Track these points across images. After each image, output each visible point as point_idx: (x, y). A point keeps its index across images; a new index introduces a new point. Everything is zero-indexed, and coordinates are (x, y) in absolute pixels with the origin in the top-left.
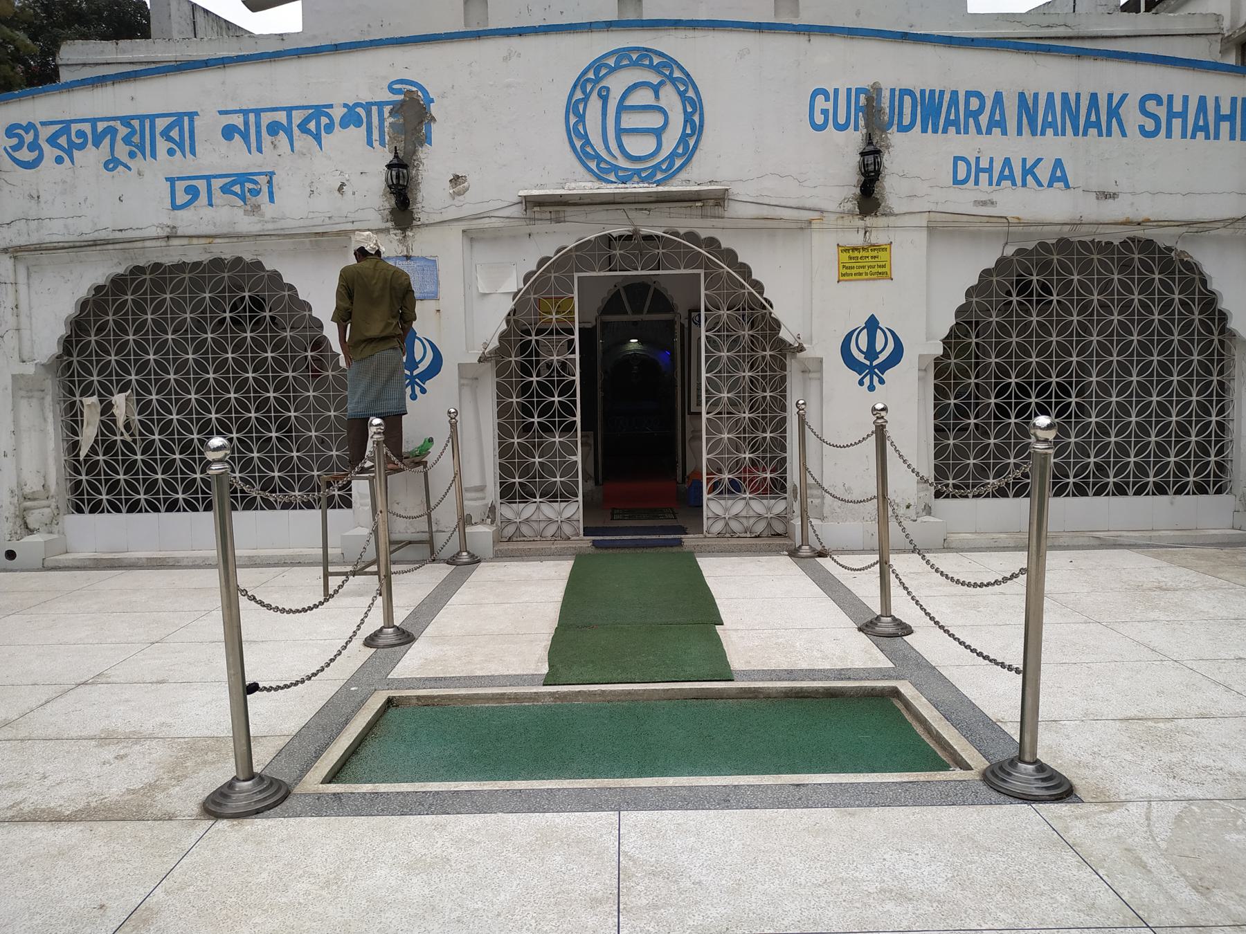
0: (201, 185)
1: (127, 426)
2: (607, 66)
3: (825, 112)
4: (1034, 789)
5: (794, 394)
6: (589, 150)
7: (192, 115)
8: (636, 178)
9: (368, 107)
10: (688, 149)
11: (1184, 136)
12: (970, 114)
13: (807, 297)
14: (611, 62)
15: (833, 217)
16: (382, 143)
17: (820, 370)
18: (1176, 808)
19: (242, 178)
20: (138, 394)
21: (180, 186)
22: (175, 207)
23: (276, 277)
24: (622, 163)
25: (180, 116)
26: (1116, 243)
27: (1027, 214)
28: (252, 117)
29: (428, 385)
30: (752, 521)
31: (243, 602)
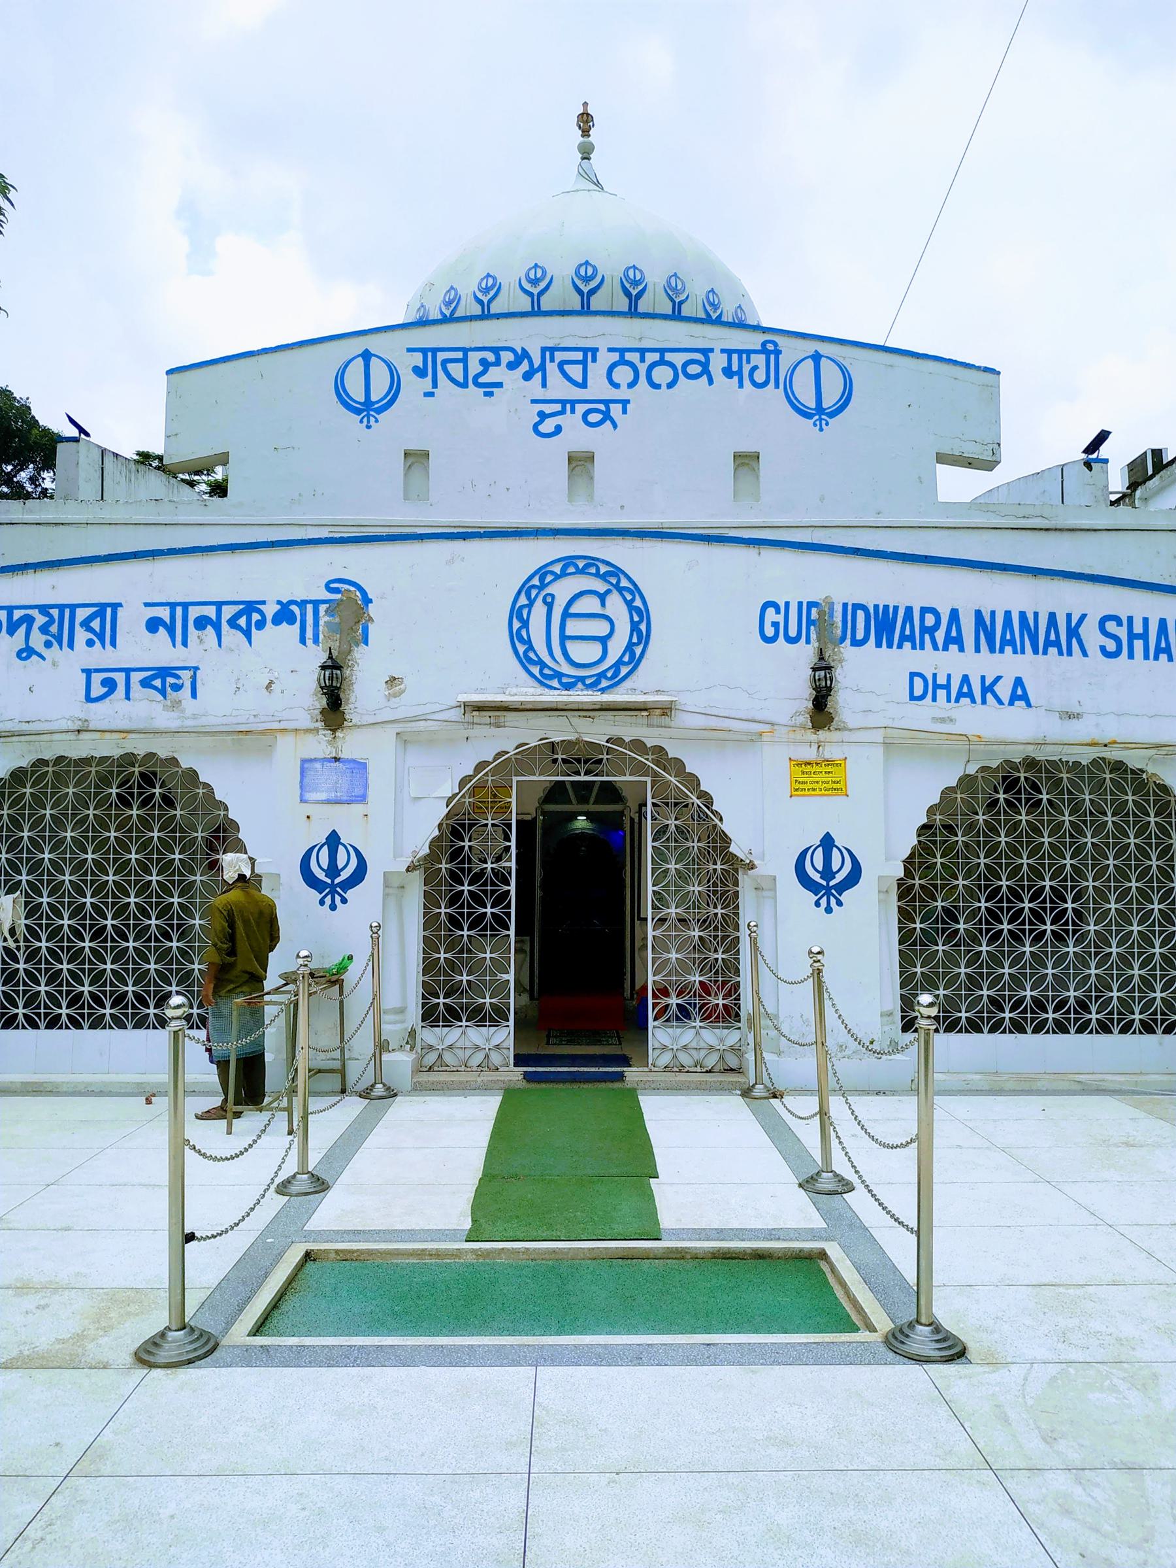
0: (120, 678)
1: (12, 931)
2: (552, 573)
3: (775, 625)
4: (930, 1350)
5: (747, 913)
6: (532, 655)
7: (115, 606)
8: (580, 685)
9: (302, 604)
10: (633, 658)
11: (1146, 657)
12: (924, 630)
13: (761, 813)
14: (557, 569)
15: (784, 730)
16: (316, 641)
17: (774, 889)
18: (1053, 1370)
19: (164, 672)
20: (27, 895)
21: (97, 678)
22: (89, 699)
23: (192, 775)
24: (566, 669)
25: (102, 607)
26: (1084, 763)
27: (988, 733)
28: (179, 610)
29: (350, 894)
30: (703, 1053)
31: (189, 1153)
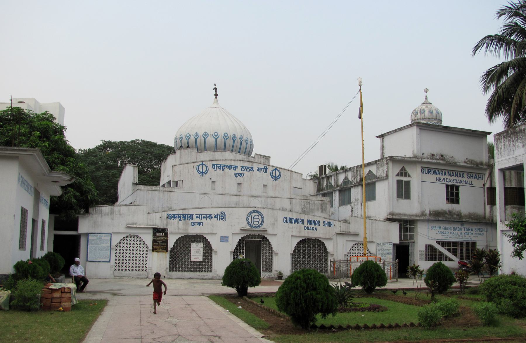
10: (262, 224)
